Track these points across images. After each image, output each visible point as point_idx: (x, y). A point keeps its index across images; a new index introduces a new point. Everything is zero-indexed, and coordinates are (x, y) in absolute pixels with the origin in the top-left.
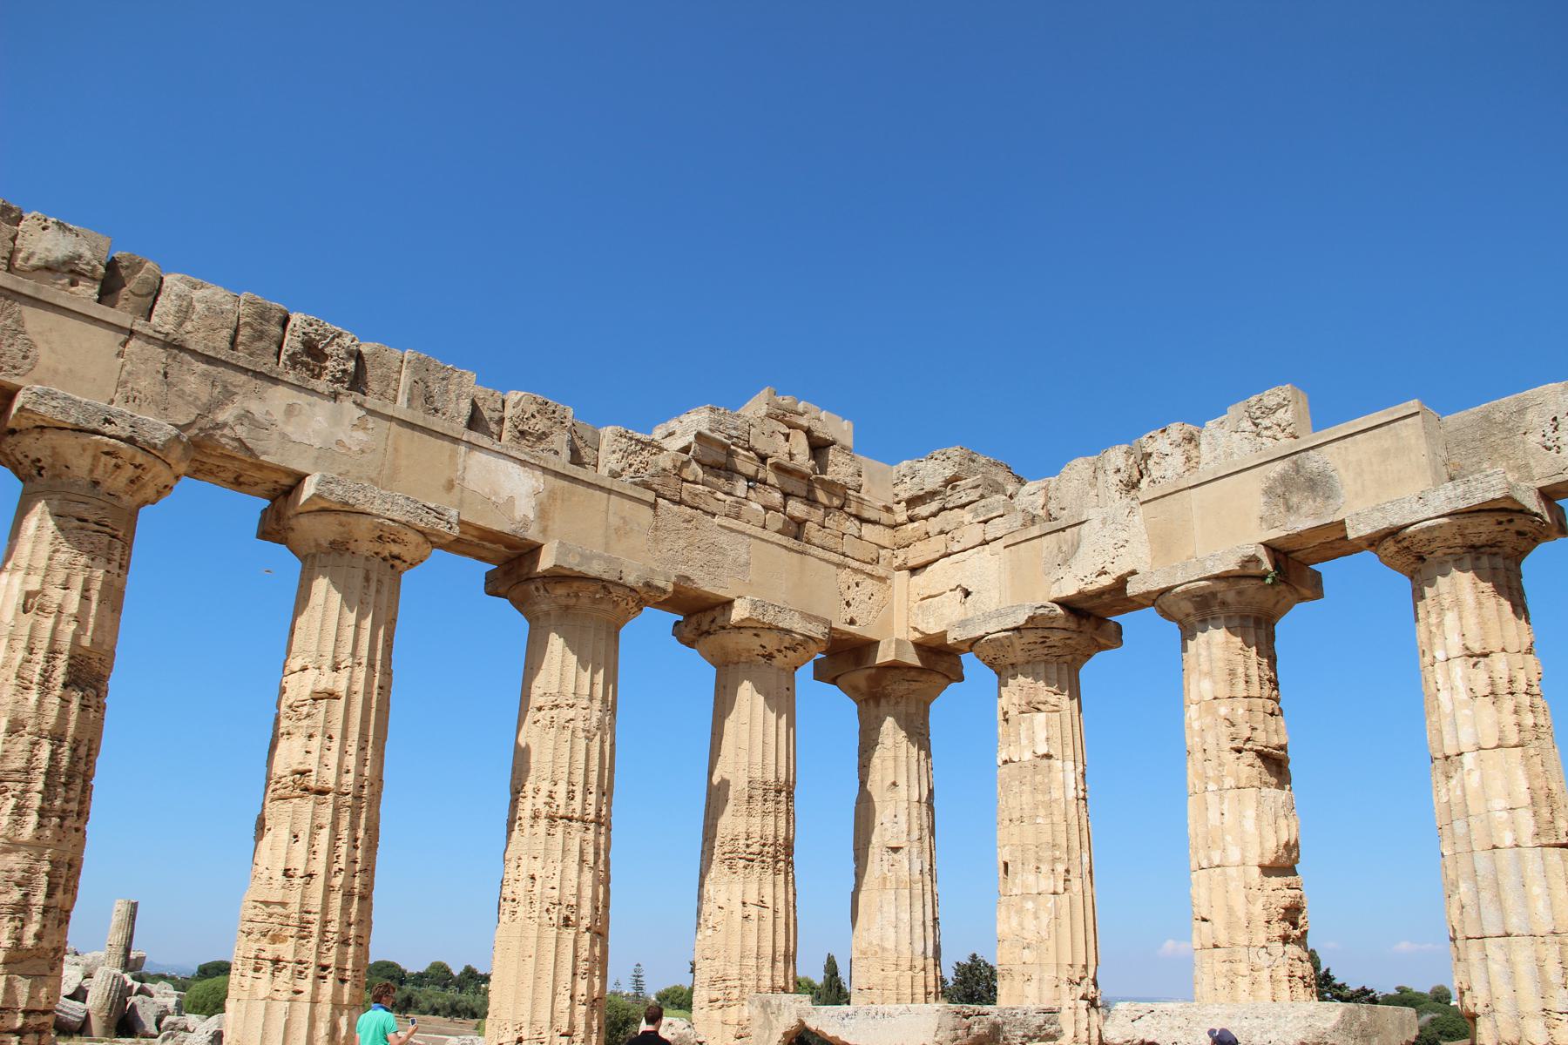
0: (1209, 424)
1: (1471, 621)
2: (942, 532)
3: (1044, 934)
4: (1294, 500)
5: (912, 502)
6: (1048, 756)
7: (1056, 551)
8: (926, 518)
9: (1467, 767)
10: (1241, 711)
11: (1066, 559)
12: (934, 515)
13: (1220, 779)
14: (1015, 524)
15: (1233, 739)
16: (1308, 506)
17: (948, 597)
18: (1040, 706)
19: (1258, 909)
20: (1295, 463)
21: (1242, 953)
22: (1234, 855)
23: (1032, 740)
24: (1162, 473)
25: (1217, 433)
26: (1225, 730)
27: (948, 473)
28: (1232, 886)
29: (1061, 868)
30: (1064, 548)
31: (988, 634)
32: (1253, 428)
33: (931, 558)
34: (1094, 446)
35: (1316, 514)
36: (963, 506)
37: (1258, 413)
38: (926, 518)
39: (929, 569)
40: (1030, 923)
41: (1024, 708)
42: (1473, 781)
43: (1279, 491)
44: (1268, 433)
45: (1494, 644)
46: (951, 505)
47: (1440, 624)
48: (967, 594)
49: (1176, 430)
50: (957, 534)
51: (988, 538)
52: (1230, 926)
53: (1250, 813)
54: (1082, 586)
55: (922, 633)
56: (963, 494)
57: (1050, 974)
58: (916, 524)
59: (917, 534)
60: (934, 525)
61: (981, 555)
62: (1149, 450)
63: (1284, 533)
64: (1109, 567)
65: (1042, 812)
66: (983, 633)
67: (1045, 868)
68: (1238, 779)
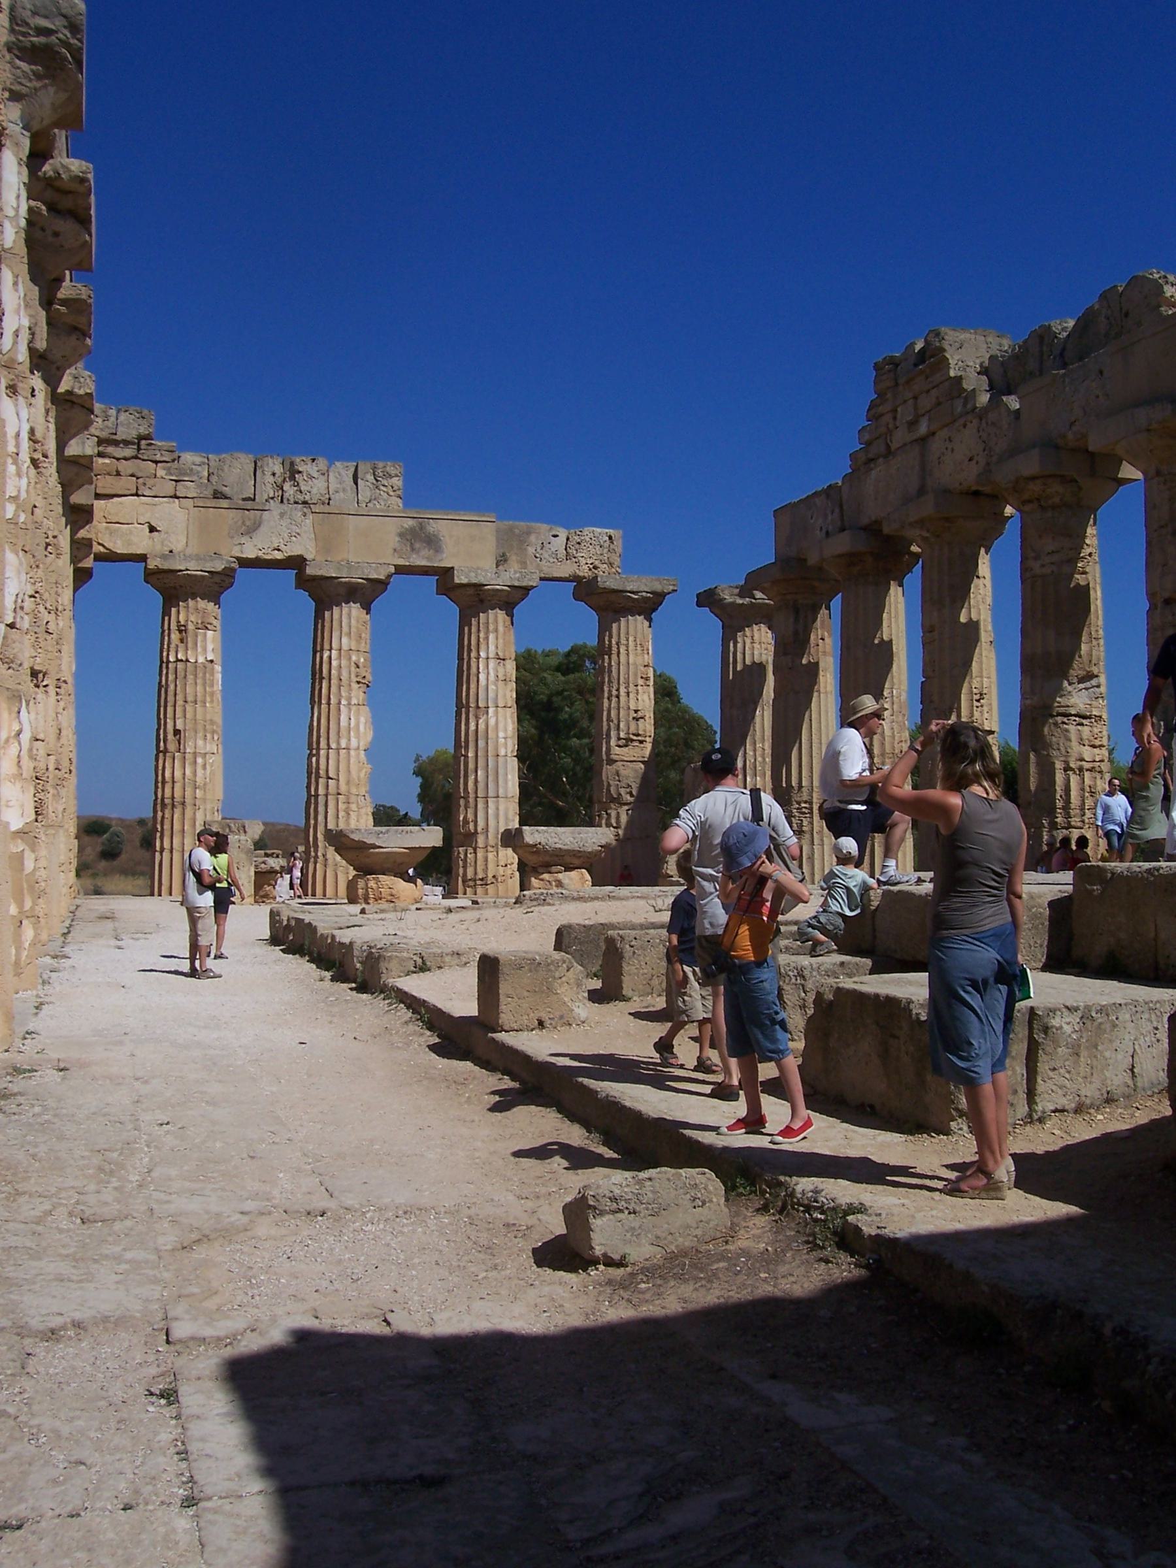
0: (338, 464)
1: (501, 641)
2: (132, 475)
3: (208, 780)
4: (417, 545)
5: (101, 442)
6: (212, 661)
7: (240, 522)
8: (118, 459)
9: (490, 715)
10: (362, 660)
11: (251, 530)
12: (126, 459)
13: (349, 699)
14: (205, 492)
15: (357, 676)
16: (425, 552)
17: (136, 528)
18: (209, 626)
19: (362, 775)
20: (421, 524)
21: (353, 799)
22: (354, 743)
23: (205, 650)
24: (308, 488)
25: (343, 472)
26: (353, 668)
27: (143, 430)
28: (352, 760)
29: (216, 738)
30: (248, 523)
31: (187, 570)
32: (374, 482)
33: (120, 493)
34: (259, 453)
35: (428, 559)
36: (156, 462)
37: (381, 474)
38: (118, 459)
39: (116, 499)
40: (200, 772)
41: (200, 626)
42: (492, 722)
43: (408, 537)
44: (384, 489)
45: (507, 657)
46: (146, 458)
47: (487, 638)
48: (152, 529)
49: (322, 463)
50: (150, 482)
51: (178, 494)
52: (348, 783)
53: (362, 720)
54: (260, 554)
55: (107, 549)
56: (157, 452)
57: (209, 806)
58: (107, 461)
59: (107, 469)
60: (126, 467)
61: (172, 505)
62: (300, 469)
63: (408, 564)
64: (282, 547)
65: (208, 699)
66: (183, 568)
67: (209, 736)
68: (358, 700)
